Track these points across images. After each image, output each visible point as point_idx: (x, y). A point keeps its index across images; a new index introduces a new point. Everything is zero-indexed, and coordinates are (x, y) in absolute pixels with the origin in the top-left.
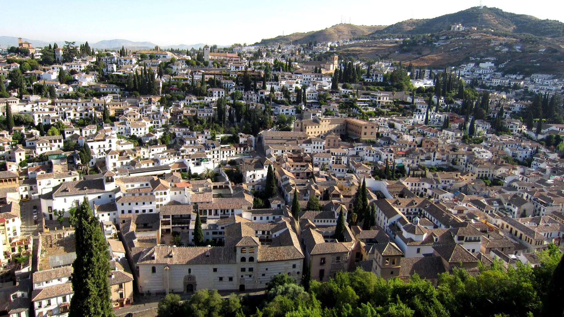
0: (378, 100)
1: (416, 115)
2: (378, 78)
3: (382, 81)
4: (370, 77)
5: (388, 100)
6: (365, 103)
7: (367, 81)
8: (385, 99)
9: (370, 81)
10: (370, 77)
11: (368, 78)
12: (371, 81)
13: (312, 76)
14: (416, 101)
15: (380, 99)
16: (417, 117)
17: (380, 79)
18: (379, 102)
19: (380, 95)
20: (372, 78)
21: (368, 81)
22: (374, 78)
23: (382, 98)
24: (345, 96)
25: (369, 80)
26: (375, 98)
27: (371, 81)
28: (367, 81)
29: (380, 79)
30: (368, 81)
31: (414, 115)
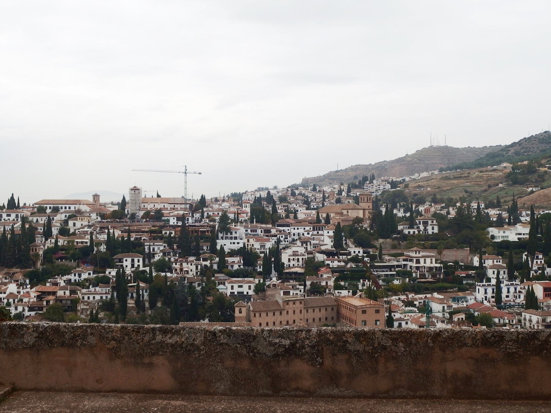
0: (414, 265)
1: (480, 288)
2: (429, 228)
3: (436, 230)
4: (416, 227)
5: (434, 265)
6: (391, 271)
7: (409, 232)
8: (428, 260)
9: (414, 232)
10: (416, 227)
11: (411, 227)
12: (417, 232)
13: (307, 228)
14: (489, 263)
15: (418, 262)
16: (482, 290)
17: (433, 229)
18: (418, 268)
19: (418, 255)
20: (418, 228)
21: (412, 233)
22: (422, 227)
23: (422, 260)
24: (355, 259)
25: (412, 231)
26: (411, 261)
27: (417, 232)
28: (409, 232)
29: (433, 229)
30: (412, 233)
31: (477, 287)
